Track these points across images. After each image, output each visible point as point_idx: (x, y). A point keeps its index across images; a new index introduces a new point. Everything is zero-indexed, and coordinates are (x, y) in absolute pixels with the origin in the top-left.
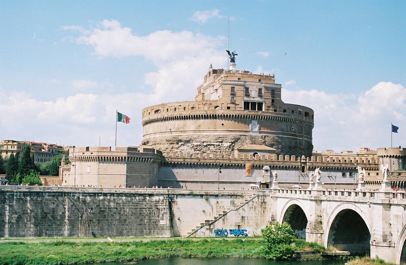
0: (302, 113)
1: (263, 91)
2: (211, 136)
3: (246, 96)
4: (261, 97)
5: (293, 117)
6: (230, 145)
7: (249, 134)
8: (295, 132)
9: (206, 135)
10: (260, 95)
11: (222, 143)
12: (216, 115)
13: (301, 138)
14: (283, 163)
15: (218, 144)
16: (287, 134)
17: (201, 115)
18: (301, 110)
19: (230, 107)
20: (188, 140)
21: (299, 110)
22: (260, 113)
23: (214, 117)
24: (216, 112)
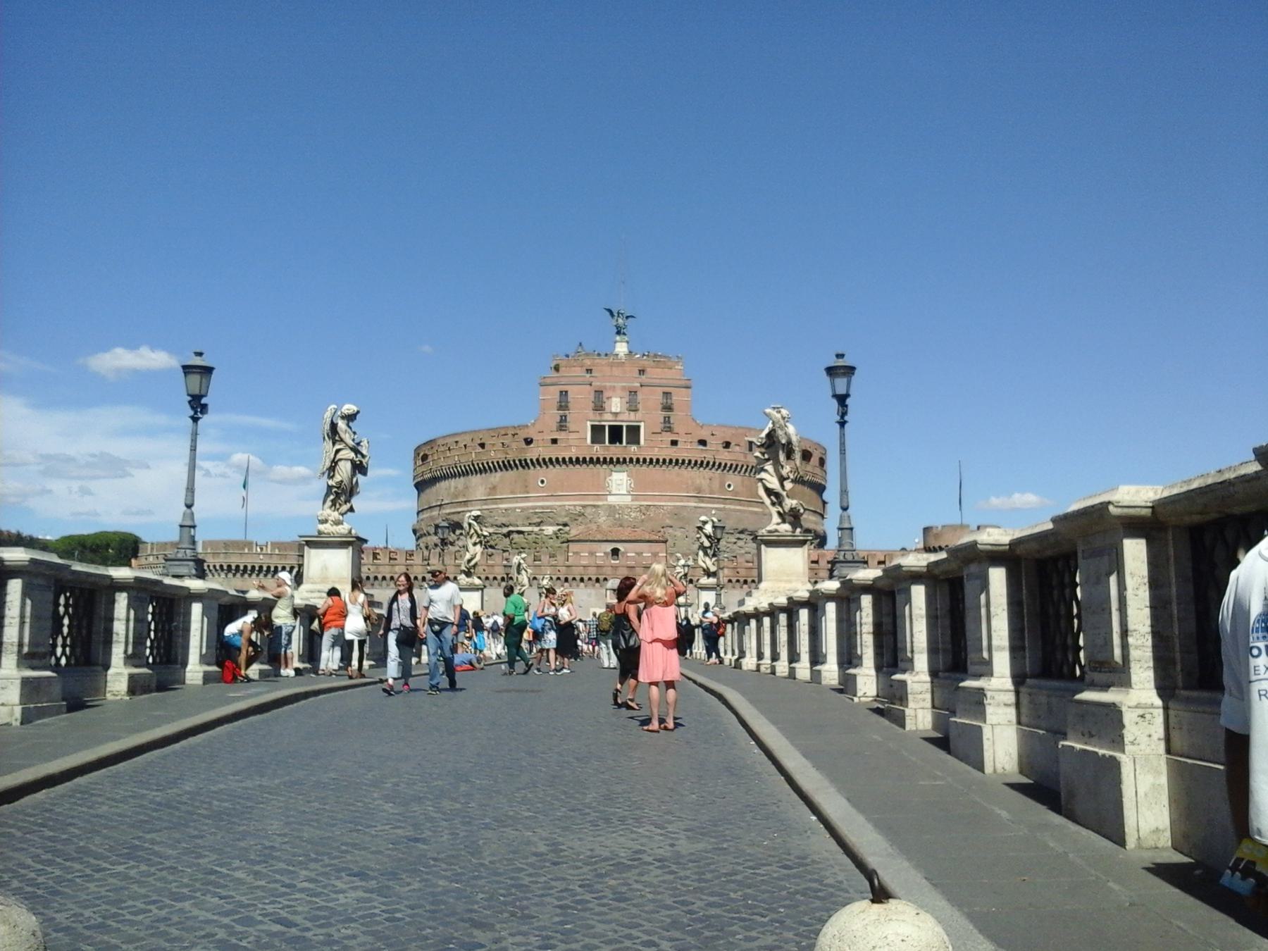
1: (640, 397)
5: (725, 457)
8: (735, 493)
10: (633, 408)
15: (529, 529)
23: (524, 464)
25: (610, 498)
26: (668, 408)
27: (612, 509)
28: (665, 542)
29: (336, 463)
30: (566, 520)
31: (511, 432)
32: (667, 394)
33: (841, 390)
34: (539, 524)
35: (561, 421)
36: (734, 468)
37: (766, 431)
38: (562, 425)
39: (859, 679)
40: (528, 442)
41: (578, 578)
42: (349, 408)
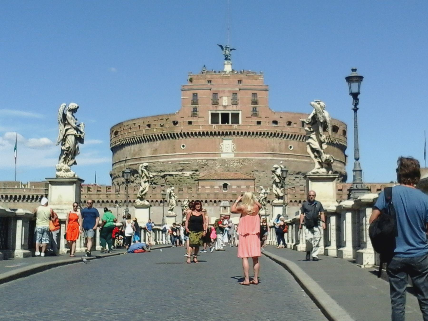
1: (239, 96)
2: (170, 163)
6: (193, 173)
7: (219, 158)
9: (163, 162)
10: (235, 103)
12: (174, 134)
16: (281, 155)
21: (300, 120)
23: (173, 136)
25: (222, 155)
26: (255, 102)
27: (223, 161)
28: (254, 180)
29: (66, 137)
30: (197, 168)
31: (165, 118)
32: (254, 95)
33: (355, 90)
34: (181, 170)
35: (194, 111)
36: (293, 137)
37: (312, 115)
38: (194, 113)
39: (364, 255)
40: (175, 123)
42: (73, 105)
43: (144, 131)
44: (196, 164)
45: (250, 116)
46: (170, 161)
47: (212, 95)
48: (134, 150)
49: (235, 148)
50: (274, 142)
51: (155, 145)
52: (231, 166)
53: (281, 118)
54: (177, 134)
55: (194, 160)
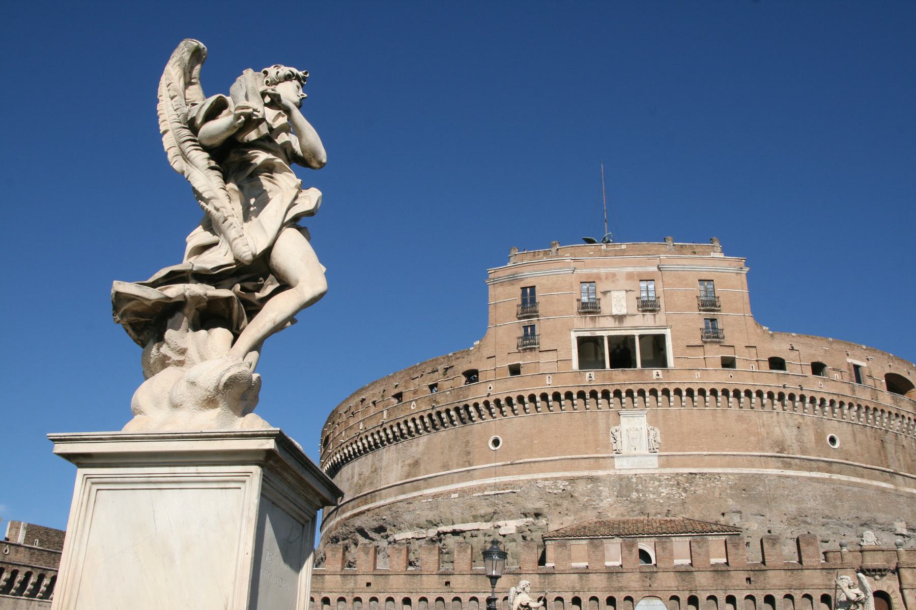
0: (867, 373)
3: (585, 313)
4: (651, 311)
7: (611, 472)
9: (435, 496)
11: (497, 520)
12: (466, 407)
13: (884, 485)
14: (748, 579)
16: (808, 465)
17: (417, 417)
18: (863, 364)
19: (519, 365)
20: (375, 524)
21: (849, 360)
22: (655, 377)
23: (464, 414)
24: (468, 396)
26: (709, 304)
27: (624, 486)
30: (539, 505)
35: (526, 336)
40: (472, 376)
41: (568, 597)
43: (385, 413)
44: (534, 493)
45: (699, 342)
46: (455, 492)
47: (577, 287)
48: (360, 475)
49: (658, 439)
50: (781, 424)
51: (414, 449)
52: (651, 496)
53: (792, 349)
54: (476, 405)
55: (529, 481)
